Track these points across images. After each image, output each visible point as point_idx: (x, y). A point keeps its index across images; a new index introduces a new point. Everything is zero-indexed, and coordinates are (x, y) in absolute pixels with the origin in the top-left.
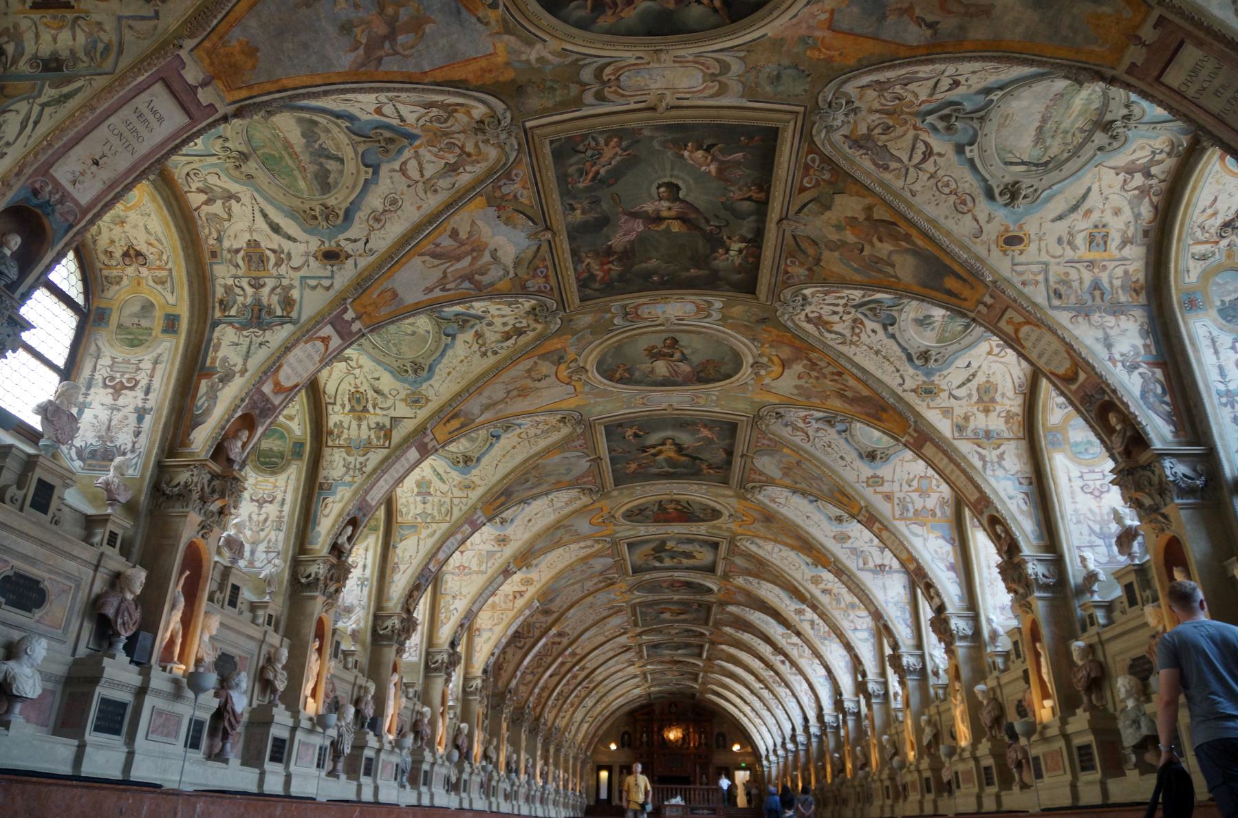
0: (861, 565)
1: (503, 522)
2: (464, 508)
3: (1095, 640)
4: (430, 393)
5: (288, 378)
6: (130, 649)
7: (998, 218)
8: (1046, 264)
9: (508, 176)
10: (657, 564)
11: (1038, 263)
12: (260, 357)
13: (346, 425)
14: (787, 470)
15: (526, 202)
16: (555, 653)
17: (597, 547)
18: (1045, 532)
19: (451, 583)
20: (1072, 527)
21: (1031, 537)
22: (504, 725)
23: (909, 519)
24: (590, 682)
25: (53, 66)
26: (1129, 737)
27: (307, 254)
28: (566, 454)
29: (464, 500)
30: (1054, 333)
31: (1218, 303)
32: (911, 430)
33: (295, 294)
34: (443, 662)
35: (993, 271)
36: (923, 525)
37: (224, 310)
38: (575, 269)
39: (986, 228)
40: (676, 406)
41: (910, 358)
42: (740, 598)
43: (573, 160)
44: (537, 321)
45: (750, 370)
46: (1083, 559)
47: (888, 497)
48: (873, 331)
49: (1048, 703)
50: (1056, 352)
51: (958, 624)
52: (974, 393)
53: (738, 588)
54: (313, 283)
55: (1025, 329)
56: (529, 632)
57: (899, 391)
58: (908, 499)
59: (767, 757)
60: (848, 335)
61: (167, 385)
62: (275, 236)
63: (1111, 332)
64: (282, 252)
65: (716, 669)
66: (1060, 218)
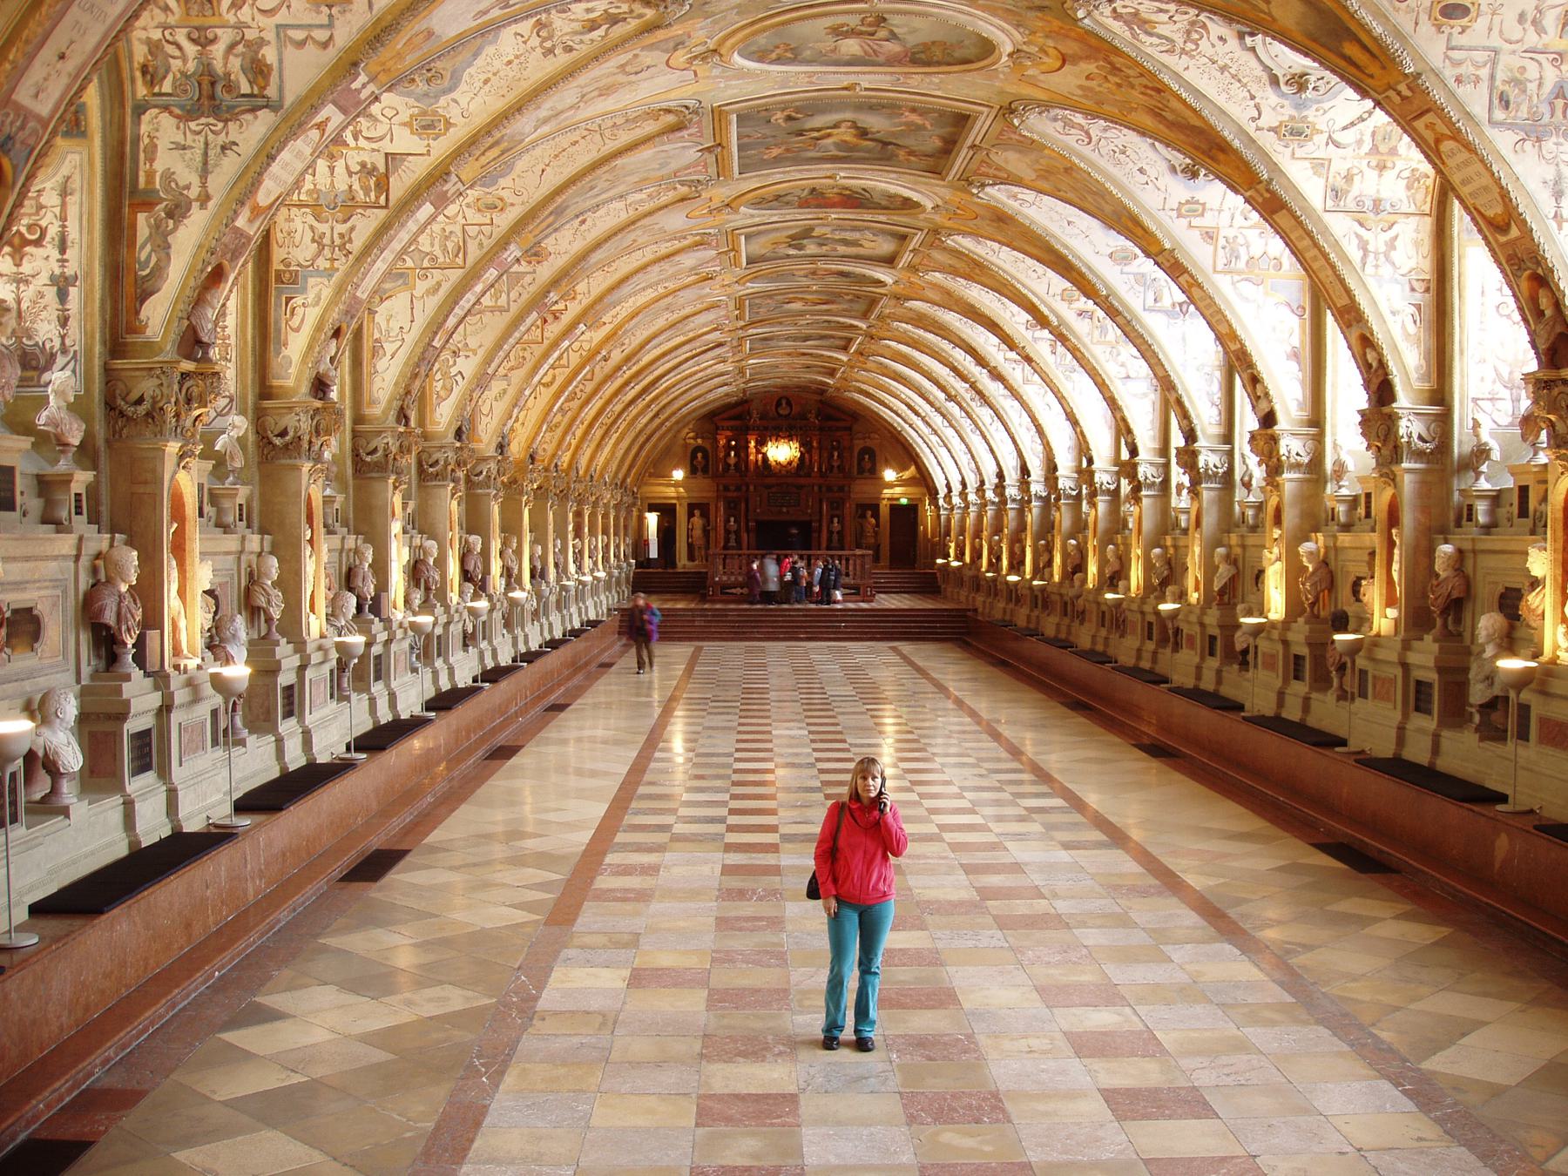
0: (1150, 302)
2: (488, 243)
3: (1467, 546)
4: (454, 114)
5: (269, 193)
8: (1496, 52)
10: (792, 252)
11: (1485, 49)
12: (227, 170)
14: (1046, 173)
16: (598, 377)
18: (1434, 369)
21: (1414, 376)
23: (1239, 273)
26: (1478, 694)
32: (1261, 187)
33: (269, 54)
34: (447, 464)
35: (1418, 57)
37: (152, 84)
41: (1274, 81)
42: (930, 294)
47: (1209, 236)
48: (1221, 38)
49: (1392, 613)
51: (1292, 446)
53: (935, 286)
54: (299, 35)
57: (1250, 128)
58: (1241, 240)
59: (948, 496)
60: (1180, 41)
61: (90, 232)
65: (869, 365)
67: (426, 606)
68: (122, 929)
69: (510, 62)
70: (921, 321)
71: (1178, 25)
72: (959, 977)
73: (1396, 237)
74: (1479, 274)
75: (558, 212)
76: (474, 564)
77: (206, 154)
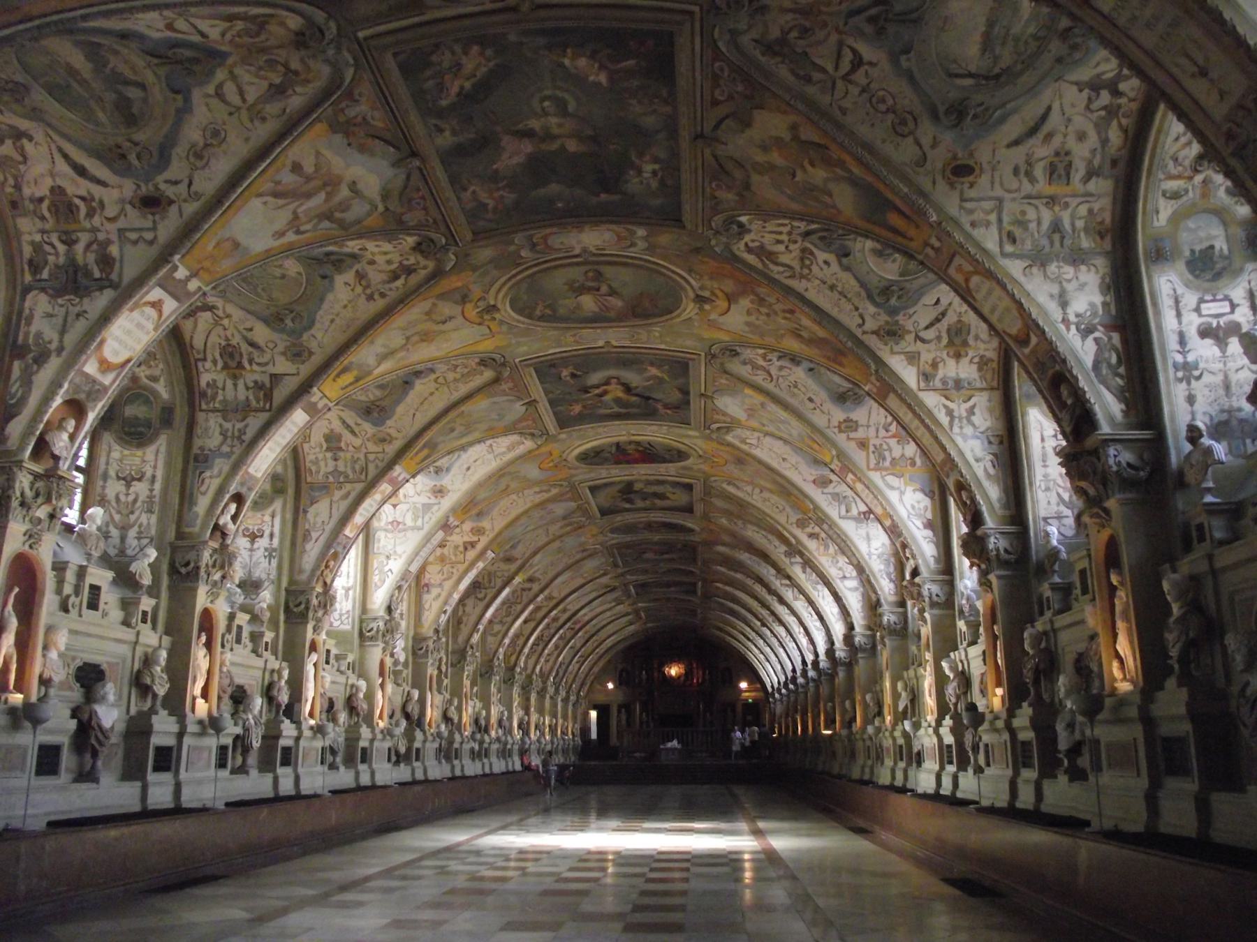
0: (843, 512)
1: (438, 471)
2: (380, 464)
4: (313, 345)
7: (943, 144)
9: (349, 95)
10: (627, 506)
11: (990, 199)
13: (220, 385)
14: (751, 412)
15: (380, 124)
16: (525, 600)
17: (554, 491)
19: (383, 541)
20: (1041, 496)
21: (997, 505)
22: (467, 683)
24: (575, 623)
27: (122, 201)
28: (495, 399)
29: (380, 456)
30: (1004, 287)
31: (1187, 253)
33: (114, 250)
35: (939, 210)
36: (900, 476)
38: (459, 199)
39: (930, 154)
40: (615, 344)
41: (870, 297)
42: (726, 538)
43: (428, 73)
44: (426, 258)
45: (691, 305)
46: (1047, 534)
47: (863, 444)
48: (826, 262)
50: (1007, 310)
52: (945, 335)
54: (133, 236)
55: (975, 280)
56: (490, 582)
57: (858, 332)
58: (885, 447)
60: (797, 268)
62: (81, 180)
63: (1070, 287)
64: (93, 199)
66: (1016, 143)
69: (345, 307)
71: (794, 254)
73: (974, 406)
75: (432, 446)
77: (65, 321)
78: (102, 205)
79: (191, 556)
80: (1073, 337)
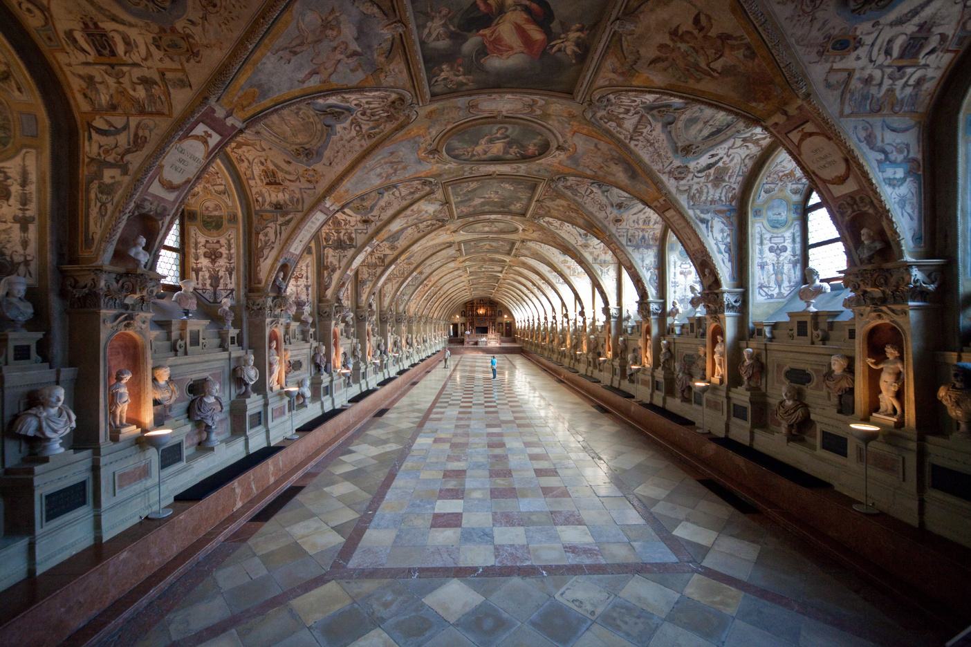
6: (326, 370)
12: (344, 261)
25: (278, 207)
26: (628, 372)
33: (353, 235)
35: (610, 231)
41: (580, 235)
47: (569, 268)
66: (635, 214)
67: (397, 352)
68: (319, 434)
70: (509, 284)
72: (506, 440)
74: (626, 276)
76: (409, 341)
78: (350, 222)
79: (363, 313)
80: (644, 271)
